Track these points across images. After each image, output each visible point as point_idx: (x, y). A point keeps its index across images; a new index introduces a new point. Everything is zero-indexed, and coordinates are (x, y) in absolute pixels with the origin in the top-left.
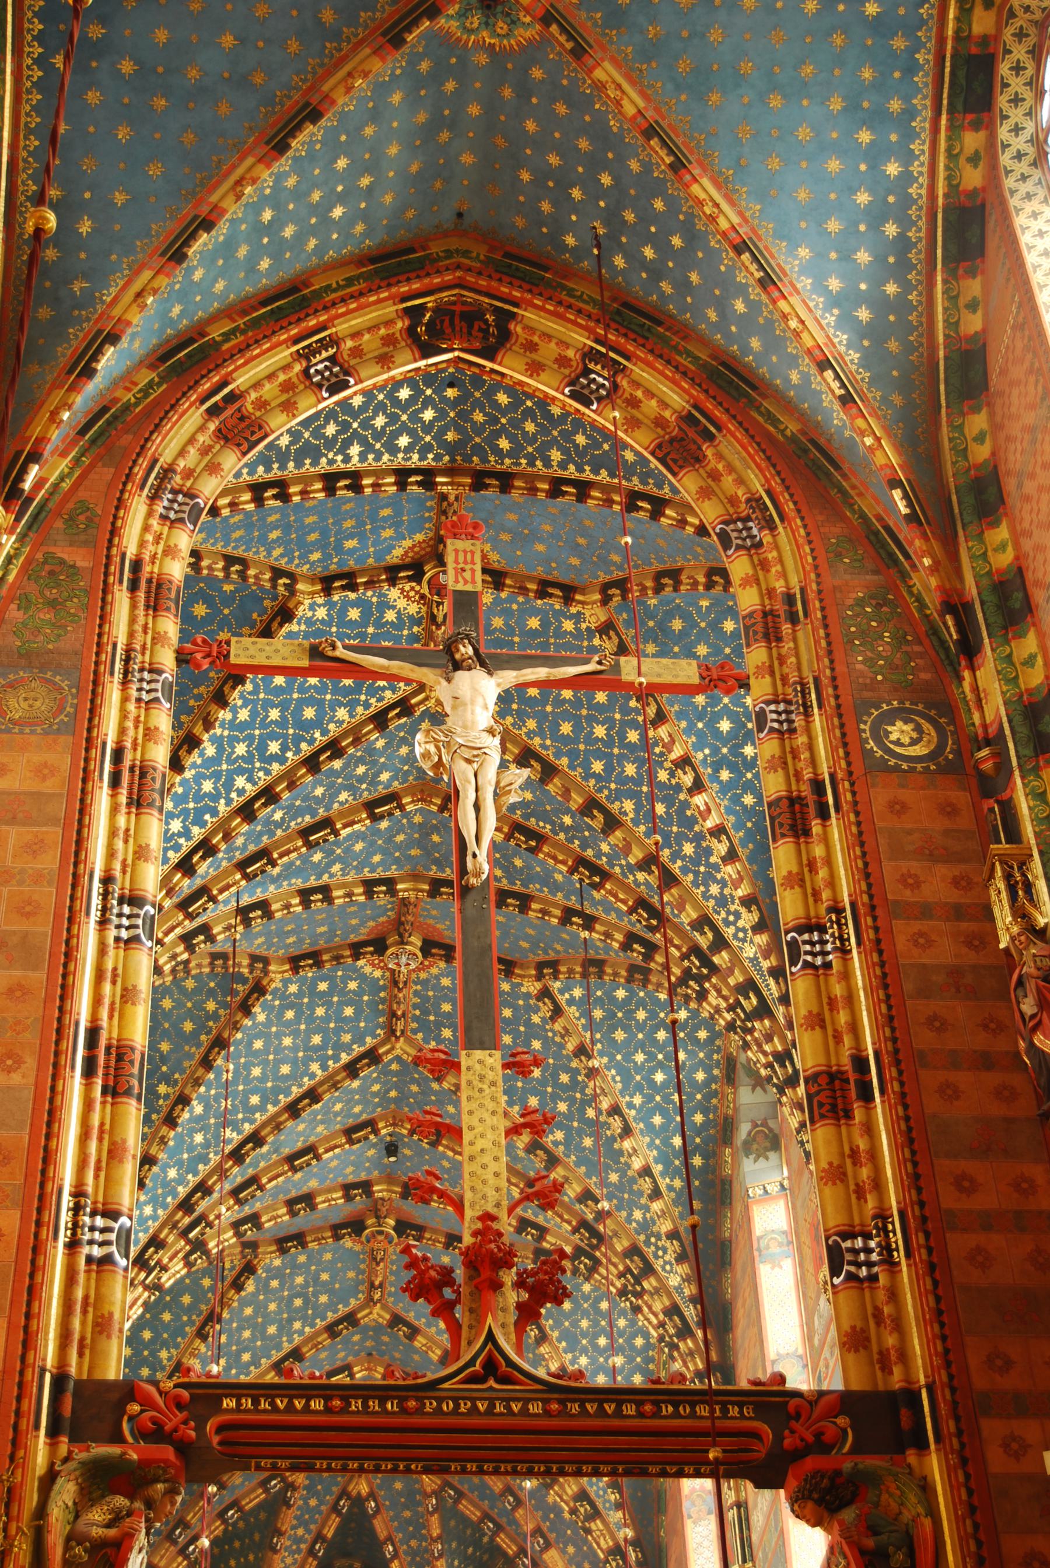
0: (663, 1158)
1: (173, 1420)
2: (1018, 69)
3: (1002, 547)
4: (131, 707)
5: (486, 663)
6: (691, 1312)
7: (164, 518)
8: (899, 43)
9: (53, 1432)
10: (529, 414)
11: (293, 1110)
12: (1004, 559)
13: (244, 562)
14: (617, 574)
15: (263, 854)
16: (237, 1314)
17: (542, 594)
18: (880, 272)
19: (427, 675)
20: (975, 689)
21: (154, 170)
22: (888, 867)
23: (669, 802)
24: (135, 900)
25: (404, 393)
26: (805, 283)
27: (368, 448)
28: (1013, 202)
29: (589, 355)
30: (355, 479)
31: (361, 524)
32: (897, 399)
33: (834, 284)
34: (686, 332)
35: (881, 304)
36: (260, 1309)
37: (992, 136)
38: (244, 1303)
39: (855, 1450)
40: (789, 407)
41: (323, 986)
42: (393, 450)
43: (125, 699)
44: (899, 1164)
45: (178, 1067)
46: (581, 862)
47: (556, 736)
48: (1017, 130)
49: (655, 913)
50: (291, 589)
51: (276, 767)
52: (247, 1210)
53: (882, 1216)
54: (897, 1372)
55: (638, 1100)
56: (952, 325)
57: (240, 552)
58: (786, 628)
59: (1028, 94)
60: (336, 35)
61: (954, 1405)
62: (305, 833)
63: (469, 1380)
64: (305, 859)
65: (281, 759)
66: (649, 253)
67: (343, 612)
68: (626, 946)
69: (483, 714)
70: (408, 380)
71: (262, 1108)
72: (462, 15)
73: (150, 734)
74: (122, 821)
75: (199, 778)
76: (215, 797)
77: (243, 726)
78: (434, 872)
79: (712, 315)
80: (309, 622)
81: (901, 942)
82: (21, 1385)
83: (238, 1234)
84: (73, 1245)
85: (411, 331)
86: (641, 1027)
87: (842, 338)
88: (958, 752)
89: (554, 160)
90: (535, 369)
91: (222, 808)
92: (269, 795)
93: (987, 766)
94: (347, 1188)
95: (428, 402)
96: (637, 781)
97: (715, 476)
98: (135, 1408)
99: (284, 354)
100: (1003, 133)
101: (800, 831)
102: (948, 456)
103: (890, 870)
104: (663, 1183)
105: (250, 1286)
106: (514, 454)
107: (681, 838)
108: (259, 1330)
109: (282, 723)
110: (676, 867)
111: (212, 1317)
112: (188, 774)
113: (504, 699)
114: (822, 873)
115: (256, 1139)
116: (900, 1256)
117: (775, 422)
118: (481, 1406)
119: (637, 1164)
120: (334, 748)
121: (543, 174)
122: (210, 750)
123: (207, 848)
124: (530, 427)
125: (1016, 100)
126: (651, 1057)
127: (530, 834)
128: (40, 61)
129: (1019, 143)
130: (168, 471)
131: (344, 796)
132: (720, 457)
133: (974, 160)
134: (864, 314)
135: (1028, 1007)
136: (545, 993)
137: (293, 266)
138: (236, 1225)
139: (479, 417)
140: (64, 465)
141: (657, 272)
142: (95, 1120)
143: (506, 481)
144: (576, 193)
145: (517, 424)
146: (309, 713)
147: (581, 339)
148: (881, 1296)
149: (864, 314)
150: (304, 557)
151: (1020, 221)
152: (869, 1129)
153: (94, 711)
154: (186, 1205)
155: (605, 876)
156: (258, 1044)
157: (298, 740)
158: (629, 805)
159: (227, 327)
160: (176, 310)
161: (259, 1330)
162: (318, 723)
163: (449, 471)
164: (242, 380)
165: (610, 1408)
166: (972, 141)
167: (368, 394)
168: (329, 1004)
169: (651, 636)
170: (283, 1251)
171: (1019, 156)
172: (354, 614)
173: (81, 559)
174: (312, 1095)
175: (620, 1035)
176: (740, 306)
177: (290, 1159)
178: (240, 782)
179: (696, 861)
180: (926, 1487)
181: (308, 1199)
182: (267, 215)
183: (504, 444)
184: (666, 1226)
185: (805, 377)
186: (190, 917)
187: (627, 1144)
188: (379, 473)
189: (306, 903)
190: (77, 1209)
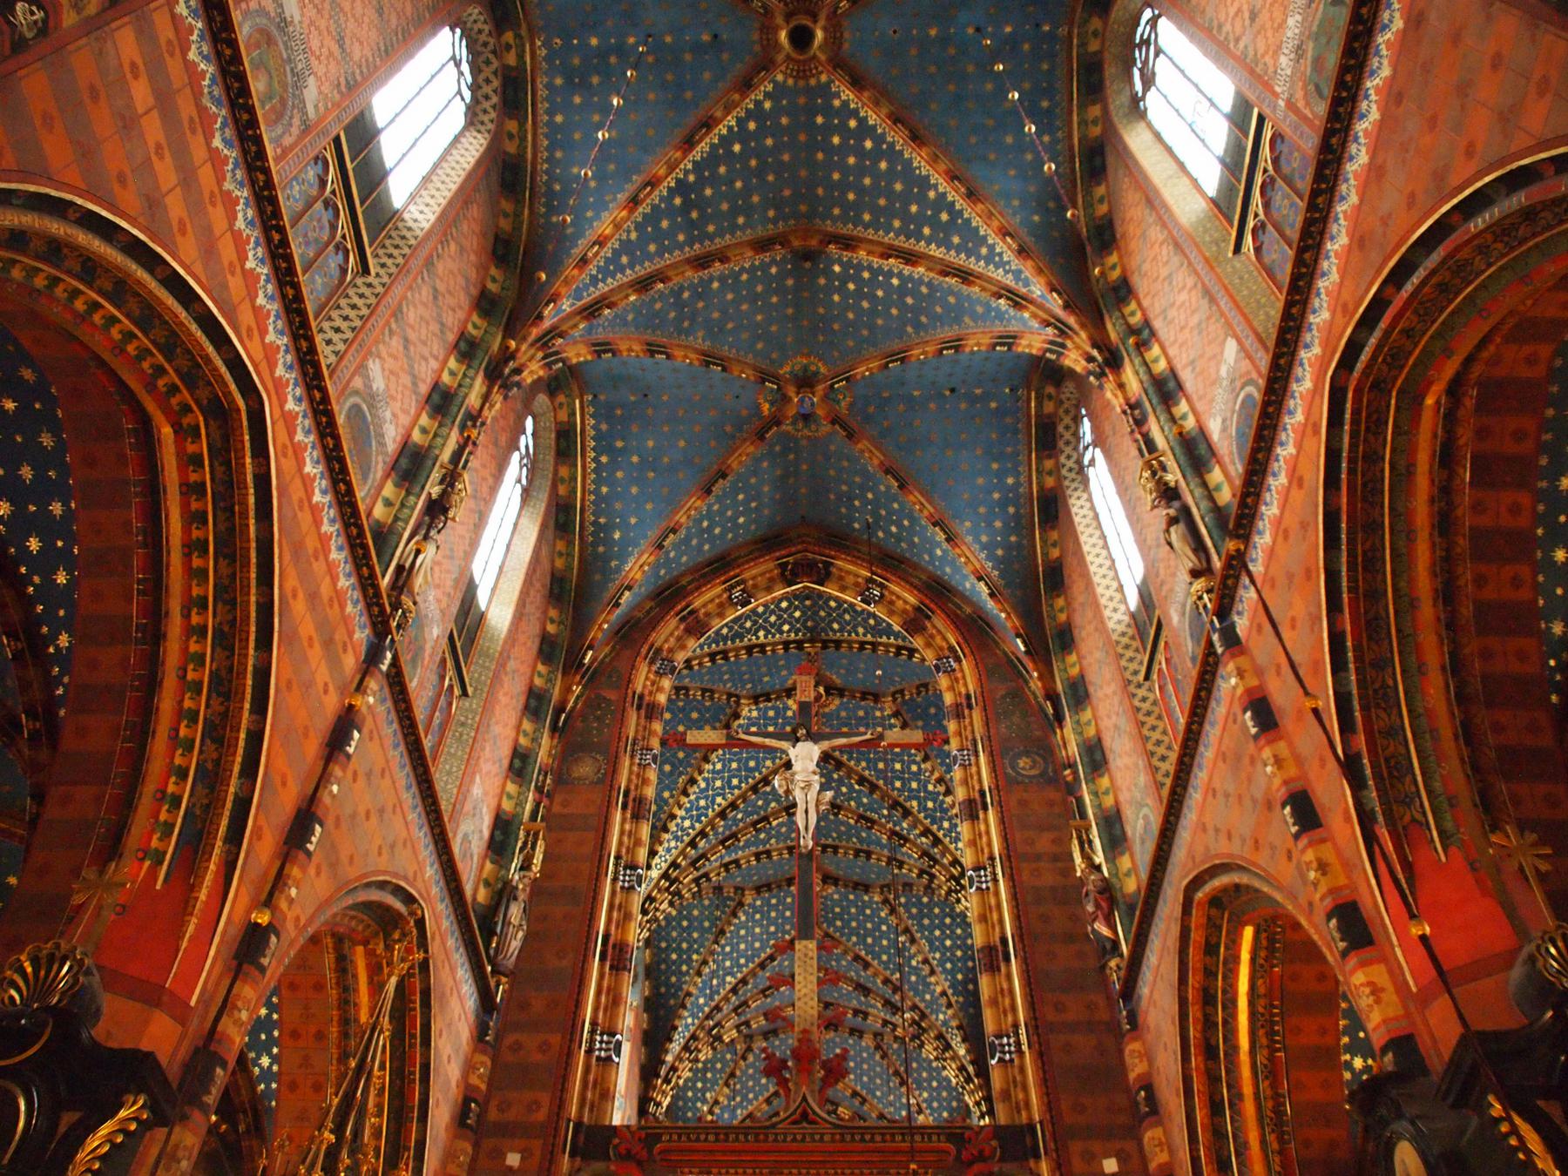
0: (952, 986)
1: (636, 1148)
2: (1067, 428)
3: (1073, 665)
4: (635, 768)
5: (814, 737)
6: (971, 1069)
7: (657, 673)
8: (1008, 420)
9: (573, 1155)
10: (845, 611)
12: (1075, 671)
13: (712, 692)
14: (899, 687)
15: (734, 836)
16: (744, 1073)
17: (863, 699)
18: (1007, 531)
19: (784, 745)
20: (1063, 738)
21: (649, 506)
22: (1018, 836)
23: (935, 801)
25: (784, 604)
26: (969, 539)
27: (768, 632)
28: (1069, 492)
29: (870, 580)
30: (762, 647)
31: (770, 669)
32: (1018, 593)
33: (984, 539)
34: (916, 566)
35: (1008, 547)
37: (1057, 462)
38: (748, 1067)
39: (1002, 1159)
40: (967, 600)
41: (774, 901)
42: (781, 632)
43: (632, 764)
44: (1024, 996)
45: (702, 946)
46: (894, 833)
47: (876, 769)
48: (1069, 457)
49: (932, 858)
50: (738, 703)
51: (736, 792)
52: (743, 1019)
53: (1016, 1026)
54: (1024, 1114)
55: (938, 955)
57: (709, 686)
58: (966, 712)
59: (1072, 439)
60: (733, 437)
61: (1054, 1134)
62: (754, 824)
63: (794, 1122)
64: (756, 837)
65: (739, 787)
66: (894, 529)
67: (765, 713)
68: (920, 876)
70: (784, 598)
71: (746, 965)
72: (794, 423)
73: (645, 781)
74: (627, 827)
75: (698, 799)
76: (707, 808)
77: (719, 772)
78: (823, 841)
79: (926, 557)
80: (749, 719)
81: (1025, 876)
82: (556, 1129)
83: (739, 1032)
84: (590, 1051)
85: (782, 574)
86: (937, 916)
88: (1055, 771)
89: (844, 488)
90: (843, 589)
91: (710, 813)
92: (733, 806)
93: (1070, 779)
95: (796, 608)
96: (918, 791)
97: (932, 636)
98: (616, 1141)
99: (719, 589)
100: (1062, 459)
102: (1047, 621)
104: (953, 999)
105: (751, 1058)
106: (841, 630)
107: (942, 819)
109: (739, 769)
110: (940, 834)
112: (692, 797)
113: (825, 757)
114: (984, 839)
115: (744, 981)
116: (1025, 1048)
117: (960, 608)
118: (799, 1137)
119: (939, 989)
121: (840, 496)
122: (703, 785)
123: (702, 834)
124: (847, 617)
125: (1068, 443)
126: (943, 932)
127: (868, 819)
128: (595, 460)
129: (1070, 464)
130: (659, 650)
131: (773, 804)
132: (934, 627)
133: (1050, 473)
135: (1090, 908)
138: (737, 1027)
139: (822, 614)
140: (607, 650)
141: (899, 539)
142: (605, 984)
143: (838, 644)
144: (857, 503)
145: (841, 616)
148: (1016, 1071)
149: (1000, 552)
150: (743, 687)
151: (1072, 501)
155: (906, 840)
156: (743, 932)
157: (747, 778)
158: (915, 803)
159: (689, 578)
160: (662, 572)
162: (757, 768)
163: (812, 641)
164: (697, 604)
165: (868, 1137)
166: (1049, 464)
167: (765, 605)
168: (777, 910)
169: (920, 717)
170: (766, 1039)
171: (1070, 470)
172: (771, 713)
173: (612, 695)
175: (926, 922)
176: (939, 552)
177: (763, 991)
178: (719, 800)
179: (950, 830)
182: (705, 524)
183: (836, 626)
184: (954, 1023)
185: (973, 585)
186: (697, 869)
187: (933, 979)
188: (775, 644)
189: (758, 859)
190: (593, 1032)
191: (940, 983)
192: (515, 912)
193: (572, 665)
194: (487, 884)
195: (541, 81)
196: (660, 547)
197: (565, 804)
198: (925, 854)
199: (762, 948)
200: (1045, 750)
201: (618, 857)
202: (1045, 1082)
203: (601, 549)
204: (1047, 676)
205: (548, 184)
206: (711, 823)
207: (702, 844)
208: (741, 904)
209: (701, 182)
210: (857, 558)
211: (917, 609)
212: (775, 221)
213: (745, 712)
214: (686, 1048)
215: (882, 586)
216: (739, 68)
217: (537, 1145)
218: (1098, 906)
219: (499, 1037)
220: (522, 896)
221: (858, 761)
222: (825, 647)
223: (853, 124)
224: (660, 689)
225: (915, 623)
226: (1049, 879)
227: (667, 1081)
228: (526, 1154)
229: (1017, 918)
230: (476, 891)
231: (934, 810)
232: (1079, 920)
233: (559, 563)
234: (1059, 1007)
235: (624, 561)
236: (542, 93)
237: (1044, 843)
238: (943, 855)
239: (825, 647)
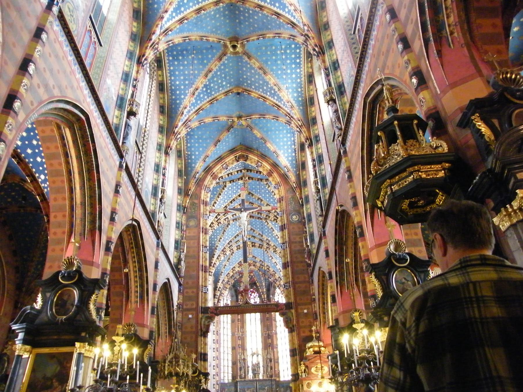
5: (246, 210)
18: (292, 153)
24: (206, 247)
26: (282, 155)
35: (292, 157)
36: (235, 257)
56: (301, 159)
69: (245, 219)
81: (293, 247)
84: (202, 292)
87: (287, 162)
103: (292, 237)
108: (236, 259)
111: (229, 259)
115: (231, 241)
120: (234, 200)
134: (290, 158)
135: (306, 256)
137: (219, 155)
143: (251, 171)
146: (230, 196)
147: (257, 159)
152: (288, 271)
153: (199, 224)
154: (223, 251)
161: (236, 259)
163: (244, 169)
174: (238, 235)
178: (222, 206)
180: (292, 313)
192: (183, 263)
193: (186, 194)
194: (176, 257)
195: (166, 58)
196: (205, 161)
197: (189, 233)
199: (235, 233)
200: (299, 213)
201: (203, 246)
202: (295, 294)
203: (190, 161)
204: (301, 193)
205: (171, 87)
207: (219, 217)
209: (210, 83)
210: (254, 155)
211: (270, 170)
212: (229, 87)
214: (218, 258)
215: (261, 163)
216: (219, 54)
217: (194, 312)
219: (183, 291)
220: (183, 259)
222: (247, 171)
223: (249, 66)
224: (207, 197)
225: (270, 174)
226: (298, 248)
227: (213, 266)
228: (192, 314)
229: (291, 257)
230: (173, 260)
232: (304, 257)
233: (180, 166)
234: (298, 278)
235: (196, 164)
236: (167, 61)
237: (298, 239)
239: (247, 171)
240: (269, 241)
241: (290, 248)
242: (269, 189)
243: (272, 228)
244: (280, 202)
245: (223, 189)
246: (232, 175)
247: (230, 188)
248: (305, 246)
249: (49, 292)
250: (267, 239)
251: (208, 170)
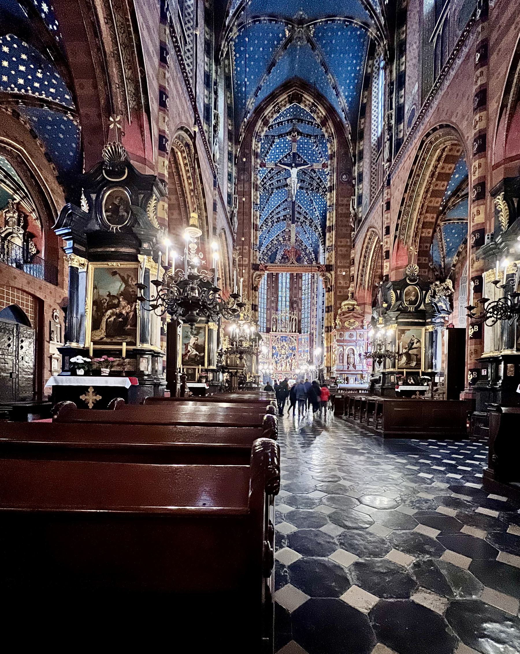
11: (277, 208)
15: (272, 177)
17: (307, 137)
27: (283, 117)
46: (311, 177)
49: (319, 185)
50: (274, 139)
62: (277, 173)
85: (289, 99)
94: (284, 216)
101: (331, 192)
135: (351, 220)
136: (307, 192)
143: (302, 121)
155: (314, 179)
174: (279, 206)
181: (279, 218)
183: (302, 115)
184: (319, 223)
191: (317, 213)
198: (318, 184)
206: (267, 175)
208: (272, 192)
213: (276, 141)
218: (353, 220)
221: (304, 156)
222: (298, 122)
229: (336, 221)
231: (321, 172)
232: (348, 221)
237: (345, 202)
238: (322, 185)
239: (298, 122)
240: (307, 214)
241: (336, 210)
242: (317, 149)
243: (311, 200)
244: (331, 159)
245: (271, 146)
246: (282, 124)
247: (278, 146)
248: (351, 209)
249: (94, 193)
250: (305, 212)
251: (259, 110)
